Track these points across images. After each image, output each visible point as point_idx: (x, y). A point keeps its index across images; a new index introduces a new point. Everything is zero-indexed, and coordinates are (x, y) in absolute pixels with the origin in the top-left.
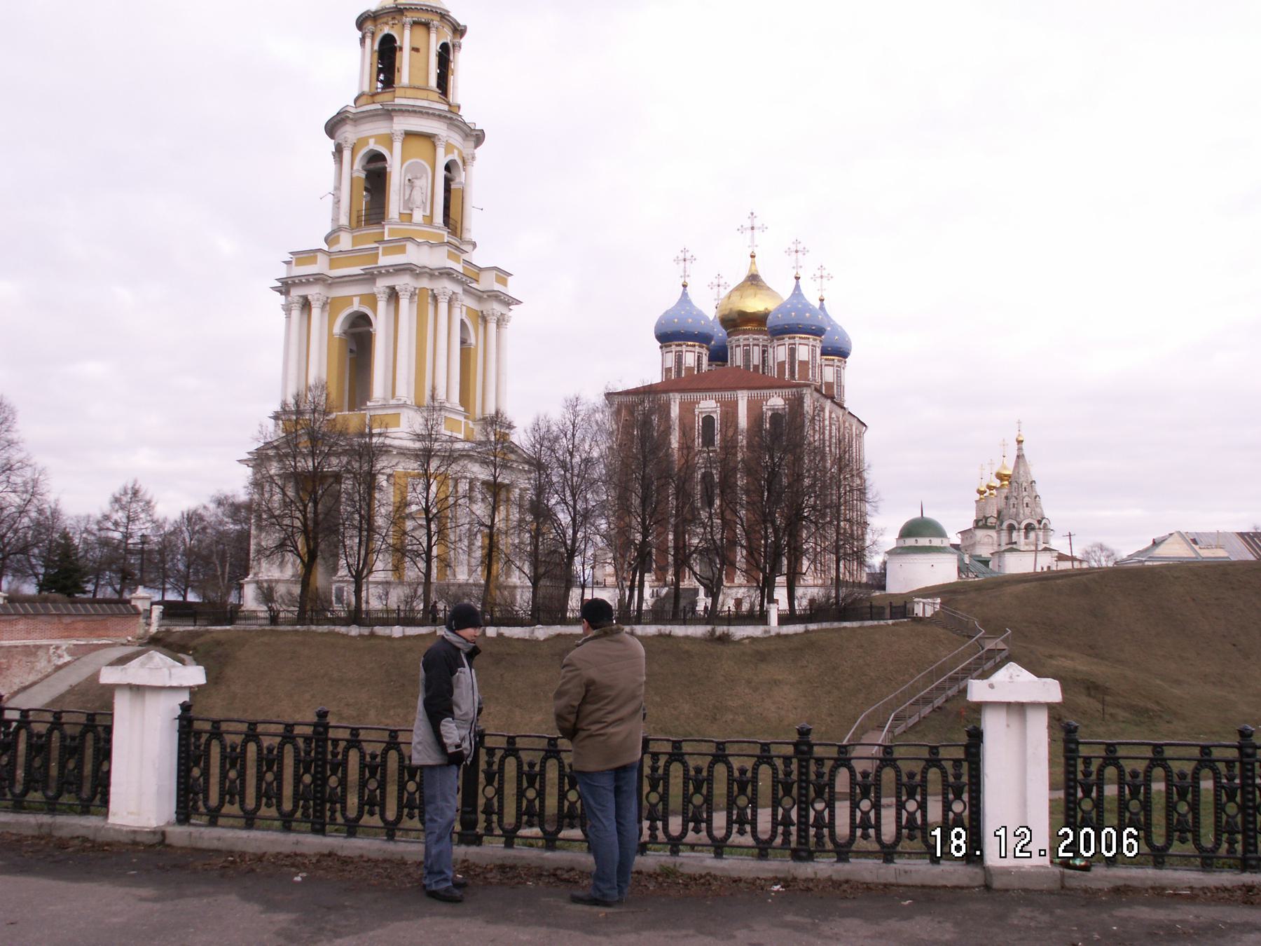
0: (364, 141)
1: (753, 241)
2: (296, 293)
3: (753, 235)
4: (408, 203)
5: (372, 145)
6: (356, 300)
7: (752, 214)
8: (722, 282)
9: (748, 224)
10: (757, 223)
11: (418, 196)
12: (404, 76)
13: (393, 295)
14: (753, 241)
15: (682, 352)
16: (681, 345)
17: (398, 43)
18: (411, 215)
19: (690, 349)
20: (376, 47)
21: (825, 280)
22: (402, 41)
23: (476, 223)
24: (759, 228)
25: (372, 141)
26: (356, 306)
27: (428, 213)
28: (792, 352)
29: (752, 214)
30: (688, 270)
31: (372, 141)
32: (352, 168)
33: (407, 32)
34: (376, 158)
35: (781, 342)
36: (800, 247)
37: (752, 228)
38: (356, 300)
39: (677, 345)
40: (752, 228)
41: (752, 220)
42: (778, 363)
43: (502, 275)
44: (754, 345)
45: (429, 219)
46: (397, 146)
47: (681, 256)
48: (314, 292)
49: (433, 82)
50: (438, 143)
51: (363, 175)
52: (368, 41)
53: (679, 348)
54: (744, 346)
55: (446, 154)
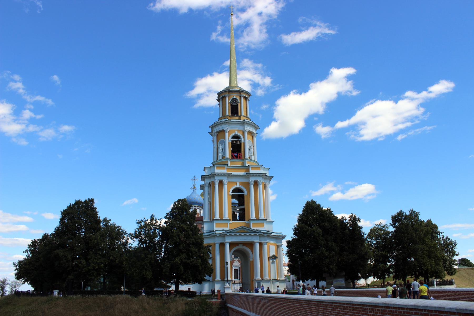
2: (217, 179)
6: (238, 184)
8: (193, 187)
13: (256, 183)
15: (196, 208)
16: (196, 206)
17: (239, 101)
19: (199, 208)
20: (230, 102)
26: (238, 185)
30: (195, 183)
31: (236, 132)
32: (228, 139)
33: (242, 99)
34: (236, 137)
39: (194, 206)
47: (193, 178)
48: (225, 180)
52: (227, 99)
53: (195, 207)
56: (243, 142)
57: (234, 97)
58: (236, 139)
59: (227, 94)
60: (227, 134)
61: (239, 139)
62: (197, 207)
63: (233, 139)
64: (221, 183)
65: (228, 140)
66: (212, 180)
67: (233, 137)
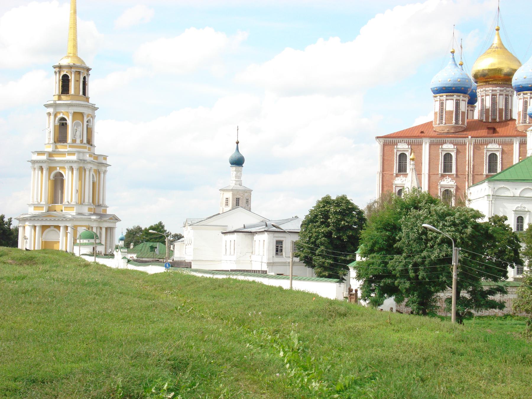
4: (74, 135)
5: (61, 116)
11: (78, 133)
12: (72, 91)
17: (70, 78)
18: (76, 140)
20: (61, 78)
22: (71, 78)
23: (96, 140)
27: (81, 139)
34: (63, 119)
38: (58, 168)
43: (105, 158)
45: (82, 142)
46: (71, 117)
49: (81, 93)
50: (84, 116)
51: (58, 124)
55: (87, 118)
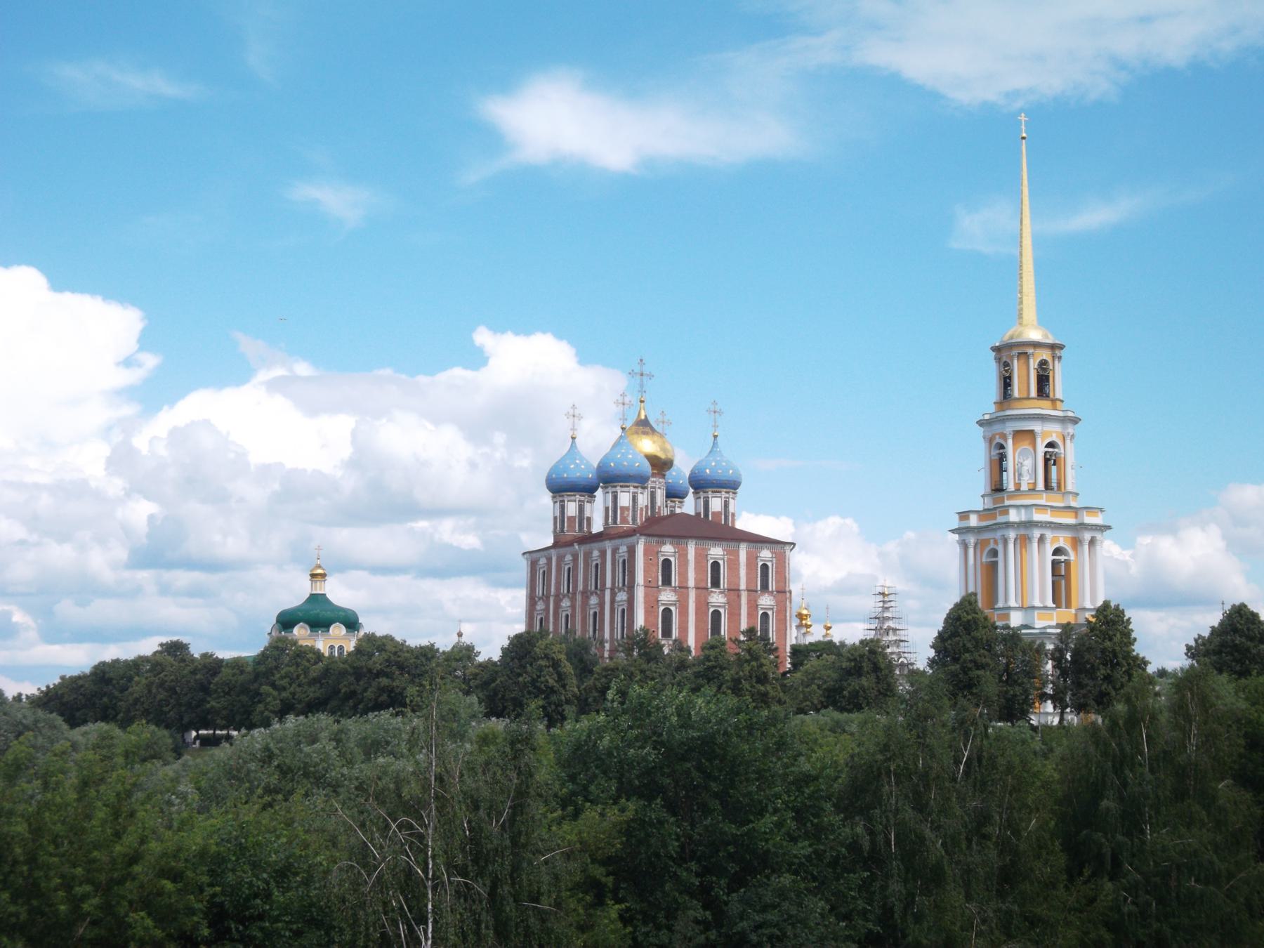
0: (1050, 433)
1: (642, 385)
3: (642, 381)
5: (1054, 438)
7: (641, 360)
9: (637, 369)
10: (646, 370)
14: (642, 385)
15: (637, 493)
21: (665, 425)
24: (648, 375)
25: (1054, 435)
28: (726, 505)
29: (641, 360)
31: (1054, 435)
34: (1051, 445)
35: (718, 494)
36: (717, 408)
37: (642, 375)
40: (642, 375)
41: (641, 366)
42: (713, 513)
44: (659, 488)
52: (1031, 361)
54: (651, 487)
56: (1063, 456)
57: (1045, 357)
58: (1050, 450)
59: (1030, 351)
60: (1039, 440)
61: (1056, 450)
62: (640, 490)
63: (1047, 449)
64: (1042, 539)
65: (1041, 449)
66: (1022, 532)
67: (1046, 446)
